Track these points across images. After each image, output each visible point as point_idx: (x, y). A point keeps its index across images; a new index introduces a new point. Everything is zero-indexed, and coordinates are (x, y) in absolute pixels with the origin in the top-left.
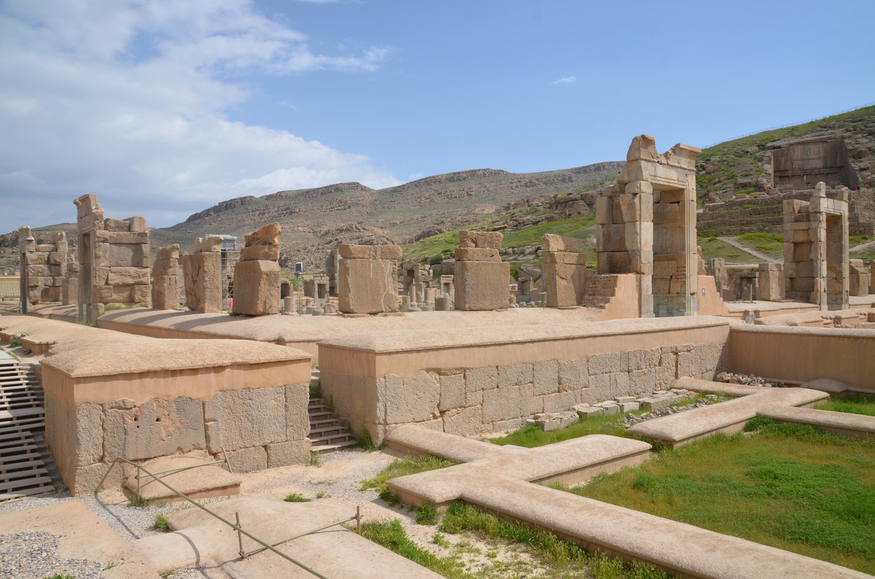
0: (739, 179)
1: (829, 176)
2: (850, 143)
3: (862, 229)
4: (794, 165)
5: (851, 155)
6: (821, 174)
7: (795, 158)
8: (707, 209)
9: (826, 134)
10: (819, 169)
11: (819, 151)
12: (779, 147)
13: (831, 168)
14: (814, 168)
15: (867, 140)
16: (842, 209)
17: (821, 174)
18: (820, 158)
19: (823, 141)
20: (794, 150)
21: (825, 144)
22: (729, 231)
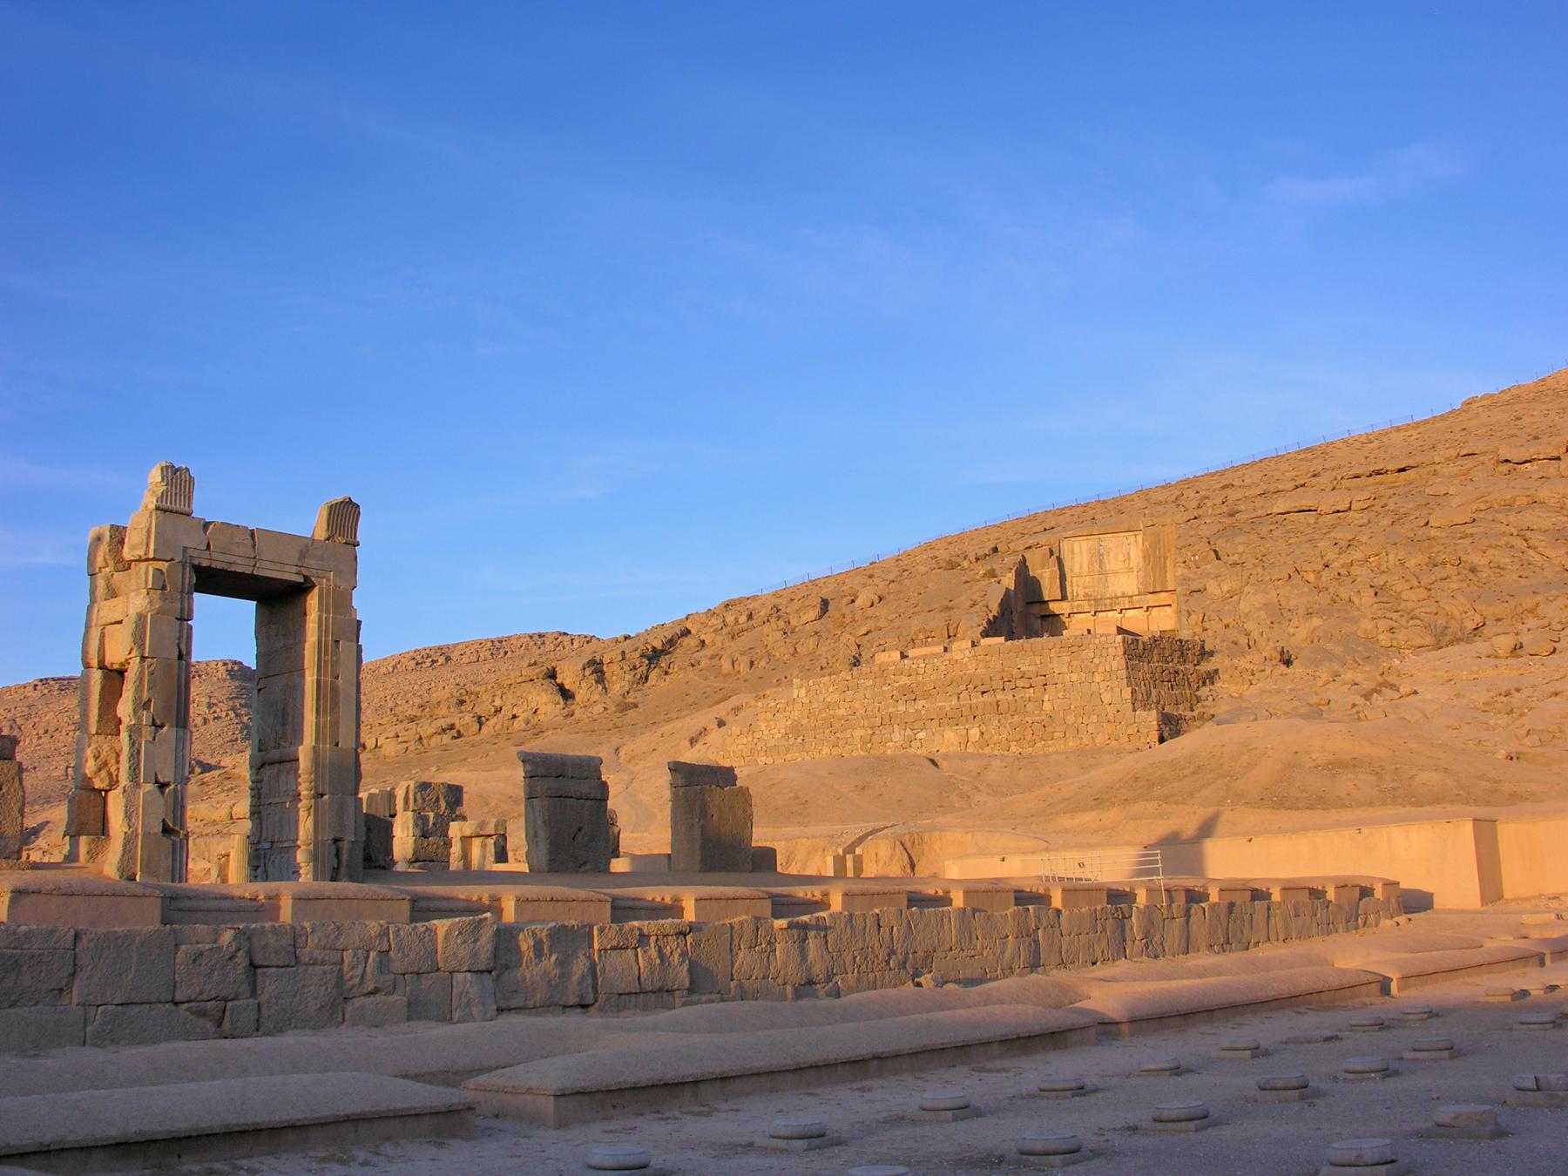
10: (1132, 596)
11: (1128, 554)
14: (1119, 594)
16: (310, 562)
18: (1130, 570)
20: (1072, 551)
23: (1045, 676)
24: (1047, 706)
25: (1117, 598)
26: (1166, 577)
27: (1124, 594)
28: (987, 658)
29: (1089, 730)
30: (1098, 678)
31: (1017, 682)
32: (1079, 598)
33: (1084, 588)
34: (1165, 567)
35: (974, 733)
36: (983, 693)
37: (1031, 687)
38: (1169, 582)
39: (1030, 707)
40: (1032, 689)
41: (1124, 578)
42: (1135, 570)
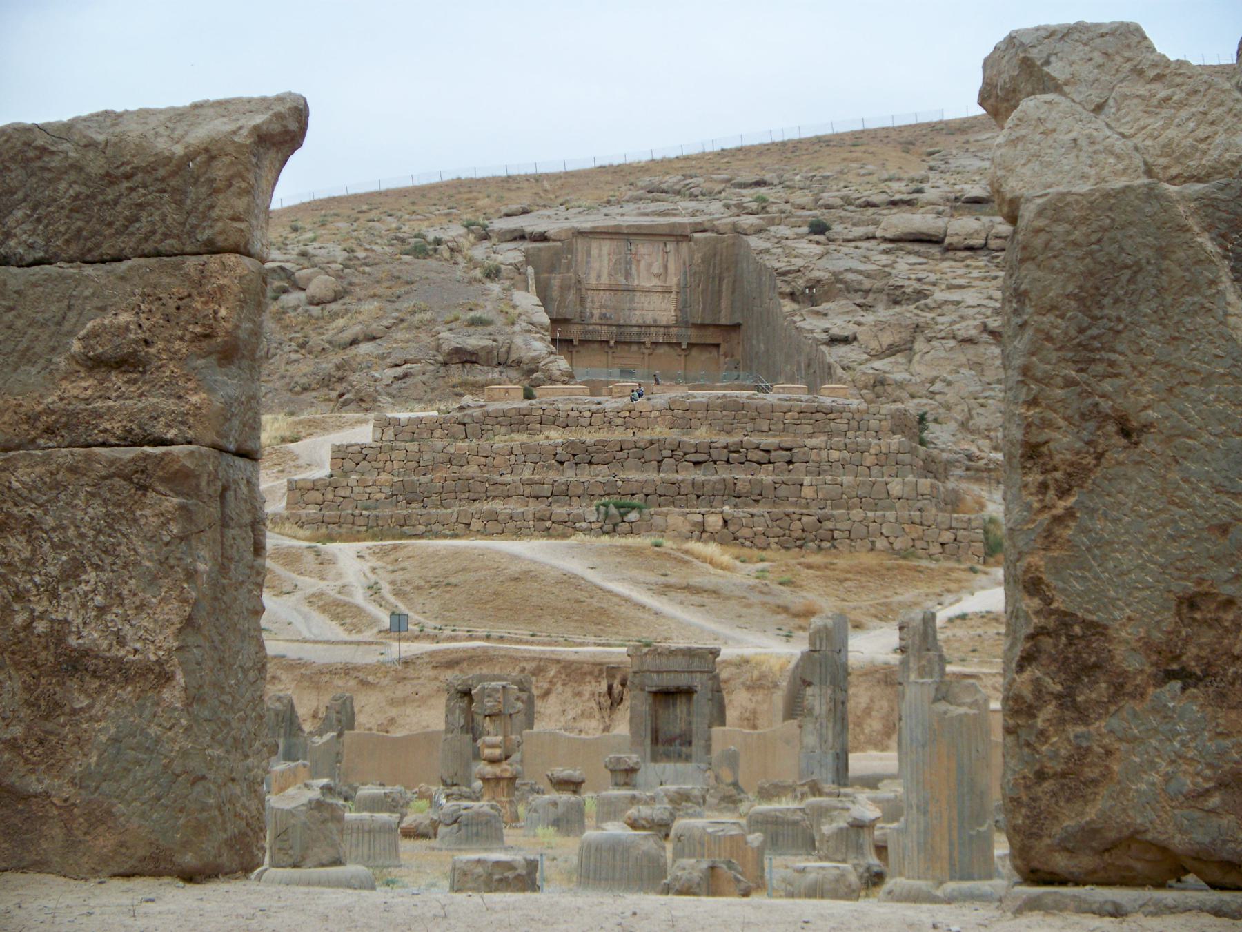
0: (445, 335)
1: (695, 352)
2: (767, 251)
3: (947, 536)
4: (589, 305)
5: (788, 290)
6: (669, 344)
7: (593, 281)
8: (390, 434)
9: (683, 212)
11: (666, 268)
12: (543, 237)
13: (702, 326)
14: (649, 321)
15: (818, 249)
17: (669, 344)
19: (678, 236)
20: (589, 254)
21: (684, 247)
22: (494, 517)
23: (790, 450)
24: (807, 492)
25: (649, 326)
26: (719, 305)
27: (655, 321)
28: (688, 415)
29: (884, 531)
30: (869, 460)
31: (750, 454)
32: (593, 321)
33: (601, 307)
34: (720, 291)
35: (714, 521)
36: (696, 463)
37: (770, 462)
38: (723, 313)
39: (783, 492)
40: (771, 467)
41: (657, 299)
42: (674, 289)
